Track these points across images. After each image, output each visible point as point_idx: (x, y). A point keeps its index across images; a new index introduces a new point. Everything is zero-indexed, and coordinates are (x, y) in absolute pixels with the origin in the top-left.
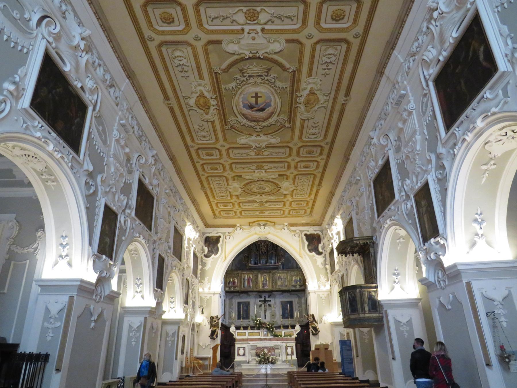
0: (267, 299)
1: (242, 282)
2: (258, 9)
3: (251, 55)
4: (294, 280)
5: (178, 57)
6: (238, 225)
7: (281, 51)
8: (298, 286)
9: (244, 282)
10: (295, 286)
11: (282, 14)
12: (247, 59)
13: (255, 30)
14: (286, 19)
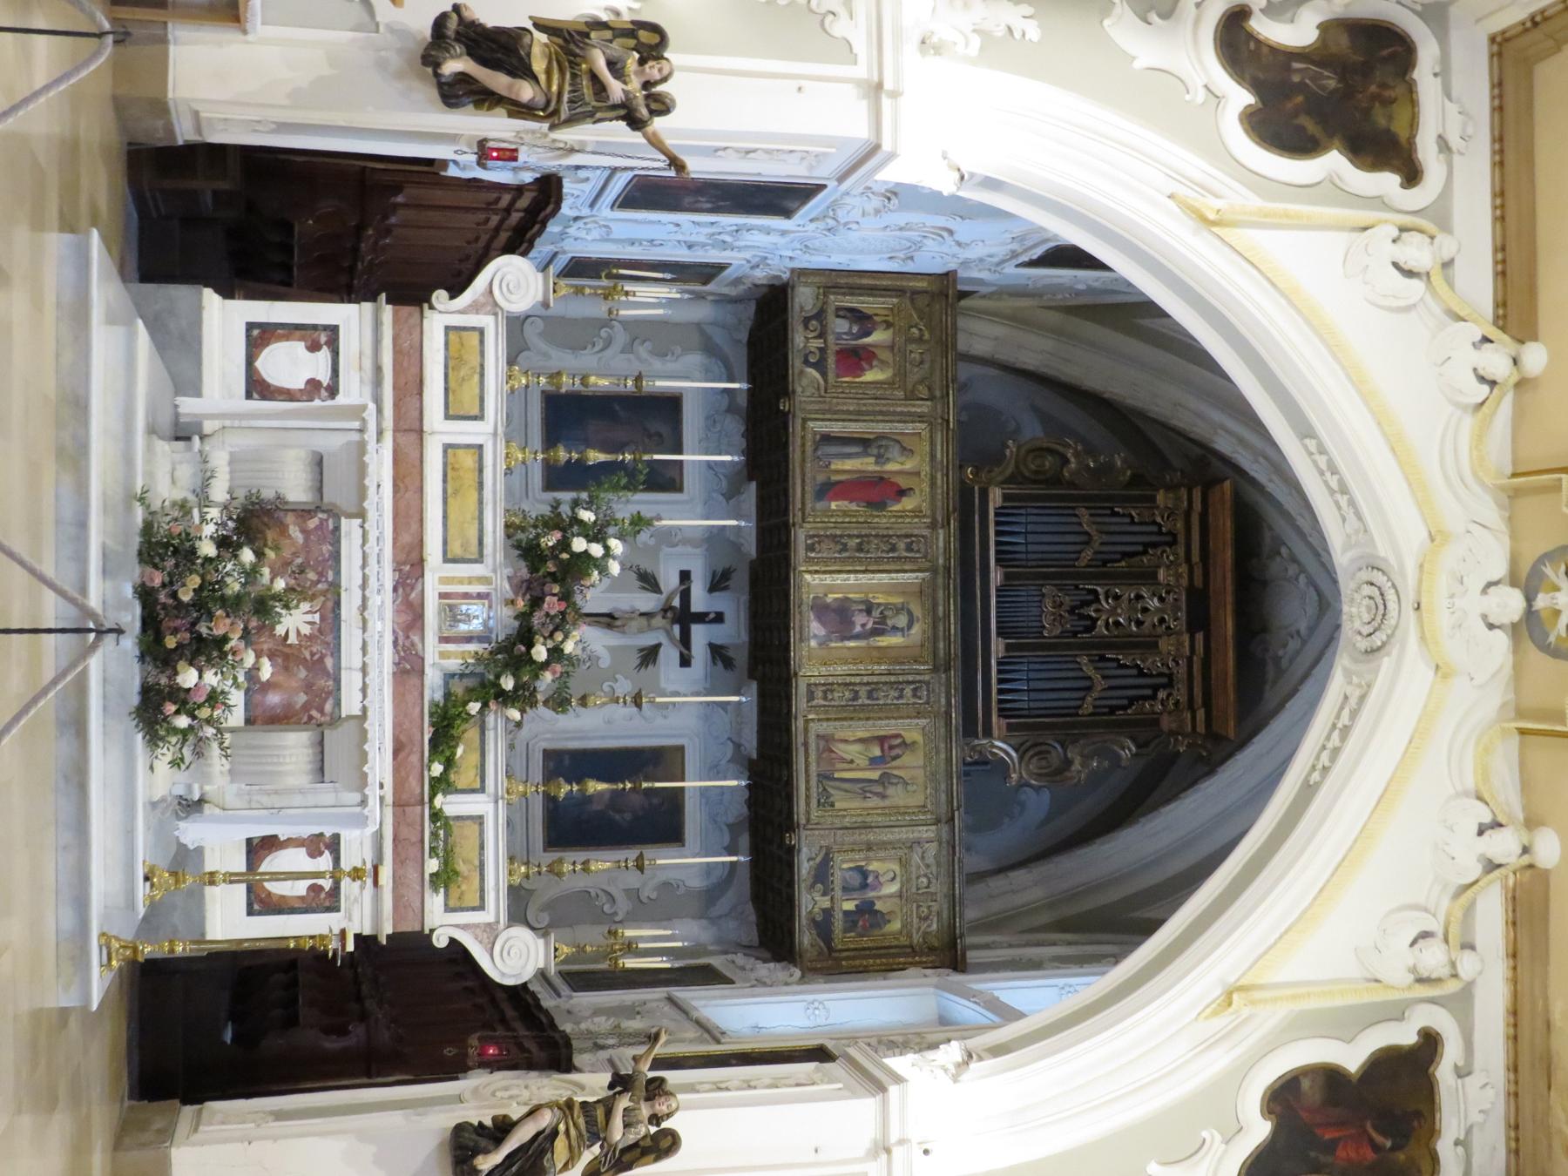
0: (699, 634)
1: (854, 428)
4: (874, 866)
6: (1535, 357)
8: (825, 903)
9: (864, 443)
10: (822, 874)
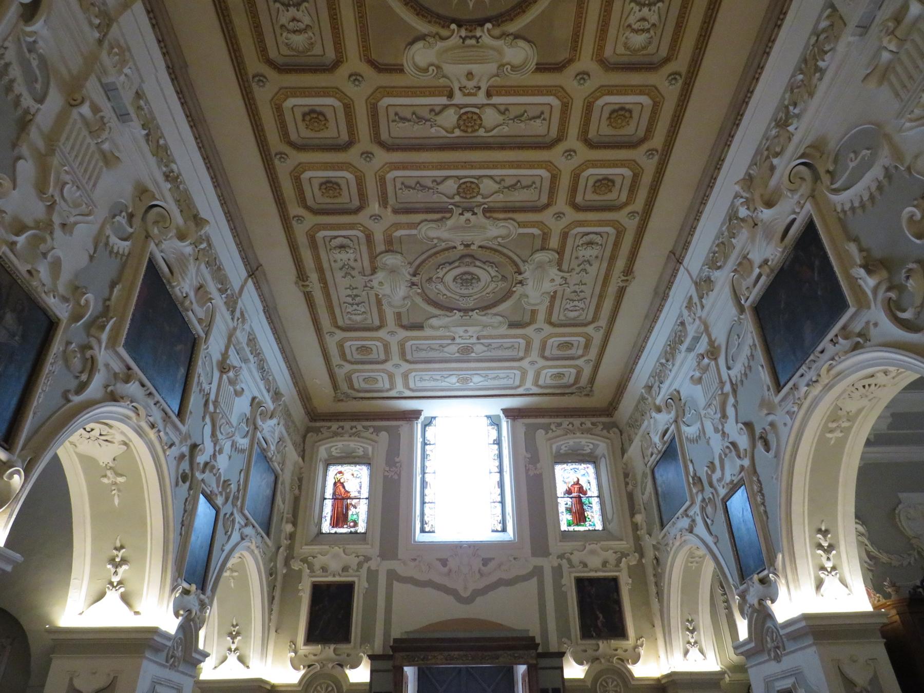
2: (457, 133)
3: (478, 33)
5: (643, 31)
7: (412, 43)
11: (416, 127)
12: (488, 20)
13: (465, 95)
14: (409, 116)
